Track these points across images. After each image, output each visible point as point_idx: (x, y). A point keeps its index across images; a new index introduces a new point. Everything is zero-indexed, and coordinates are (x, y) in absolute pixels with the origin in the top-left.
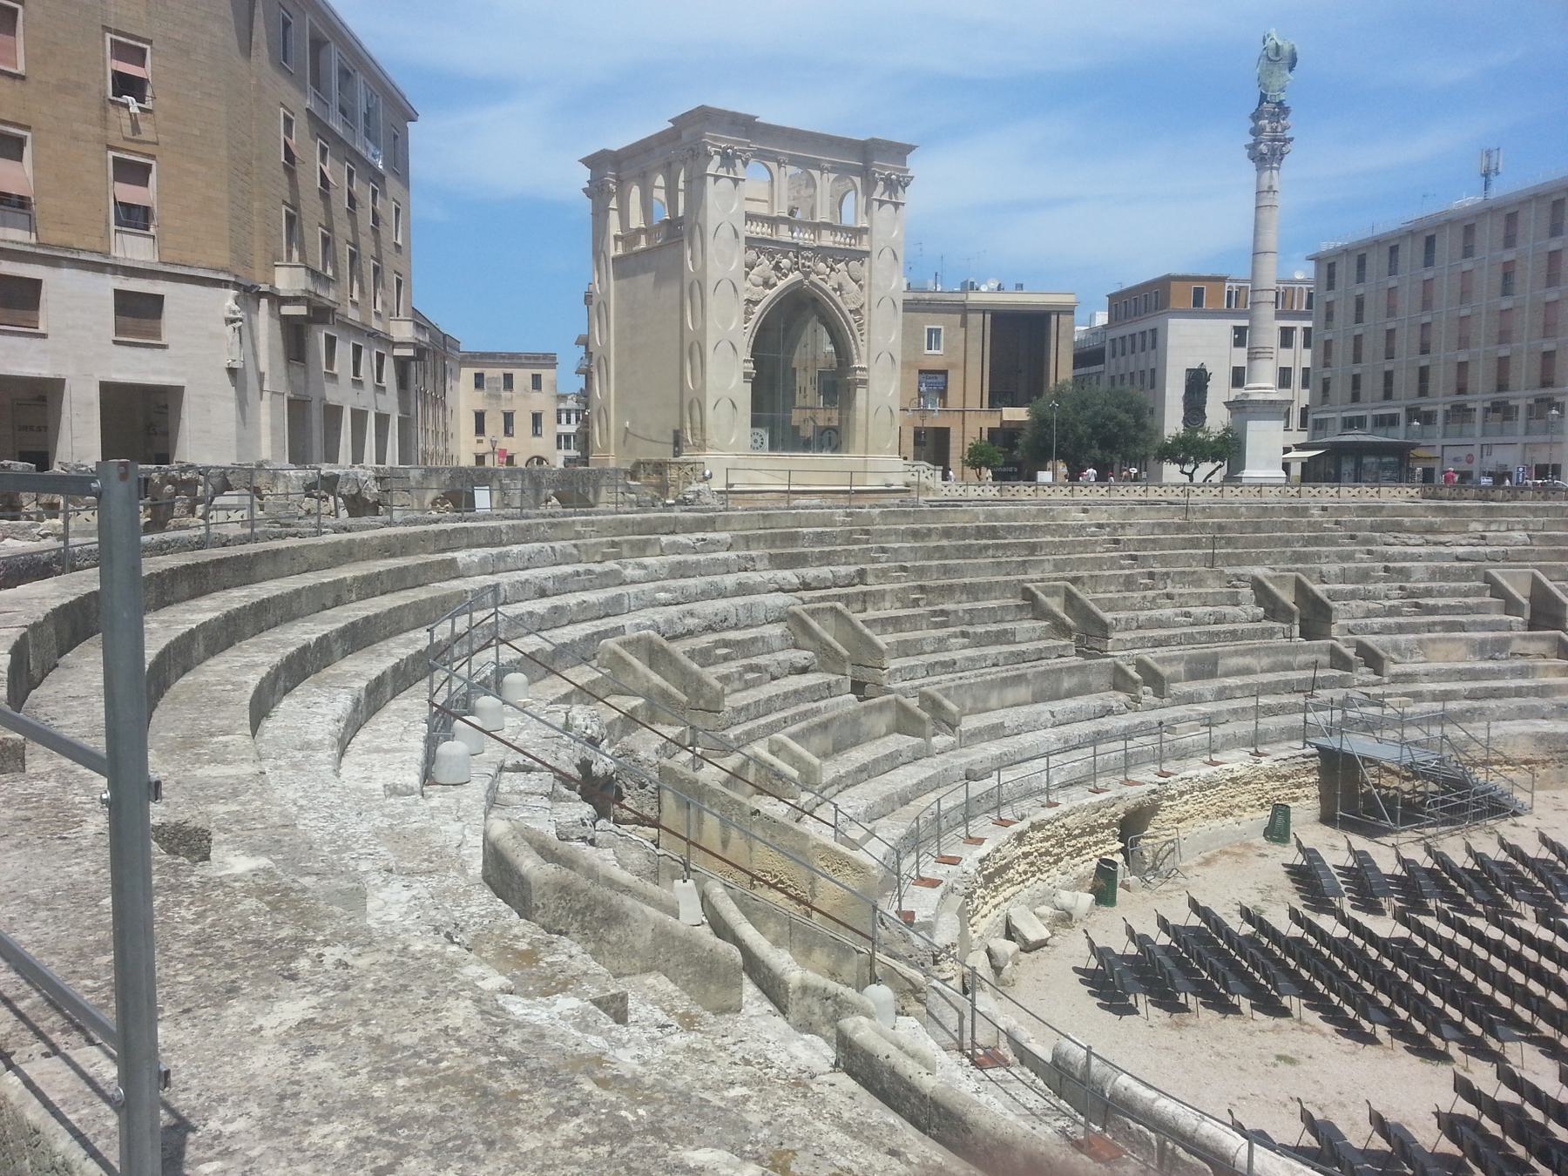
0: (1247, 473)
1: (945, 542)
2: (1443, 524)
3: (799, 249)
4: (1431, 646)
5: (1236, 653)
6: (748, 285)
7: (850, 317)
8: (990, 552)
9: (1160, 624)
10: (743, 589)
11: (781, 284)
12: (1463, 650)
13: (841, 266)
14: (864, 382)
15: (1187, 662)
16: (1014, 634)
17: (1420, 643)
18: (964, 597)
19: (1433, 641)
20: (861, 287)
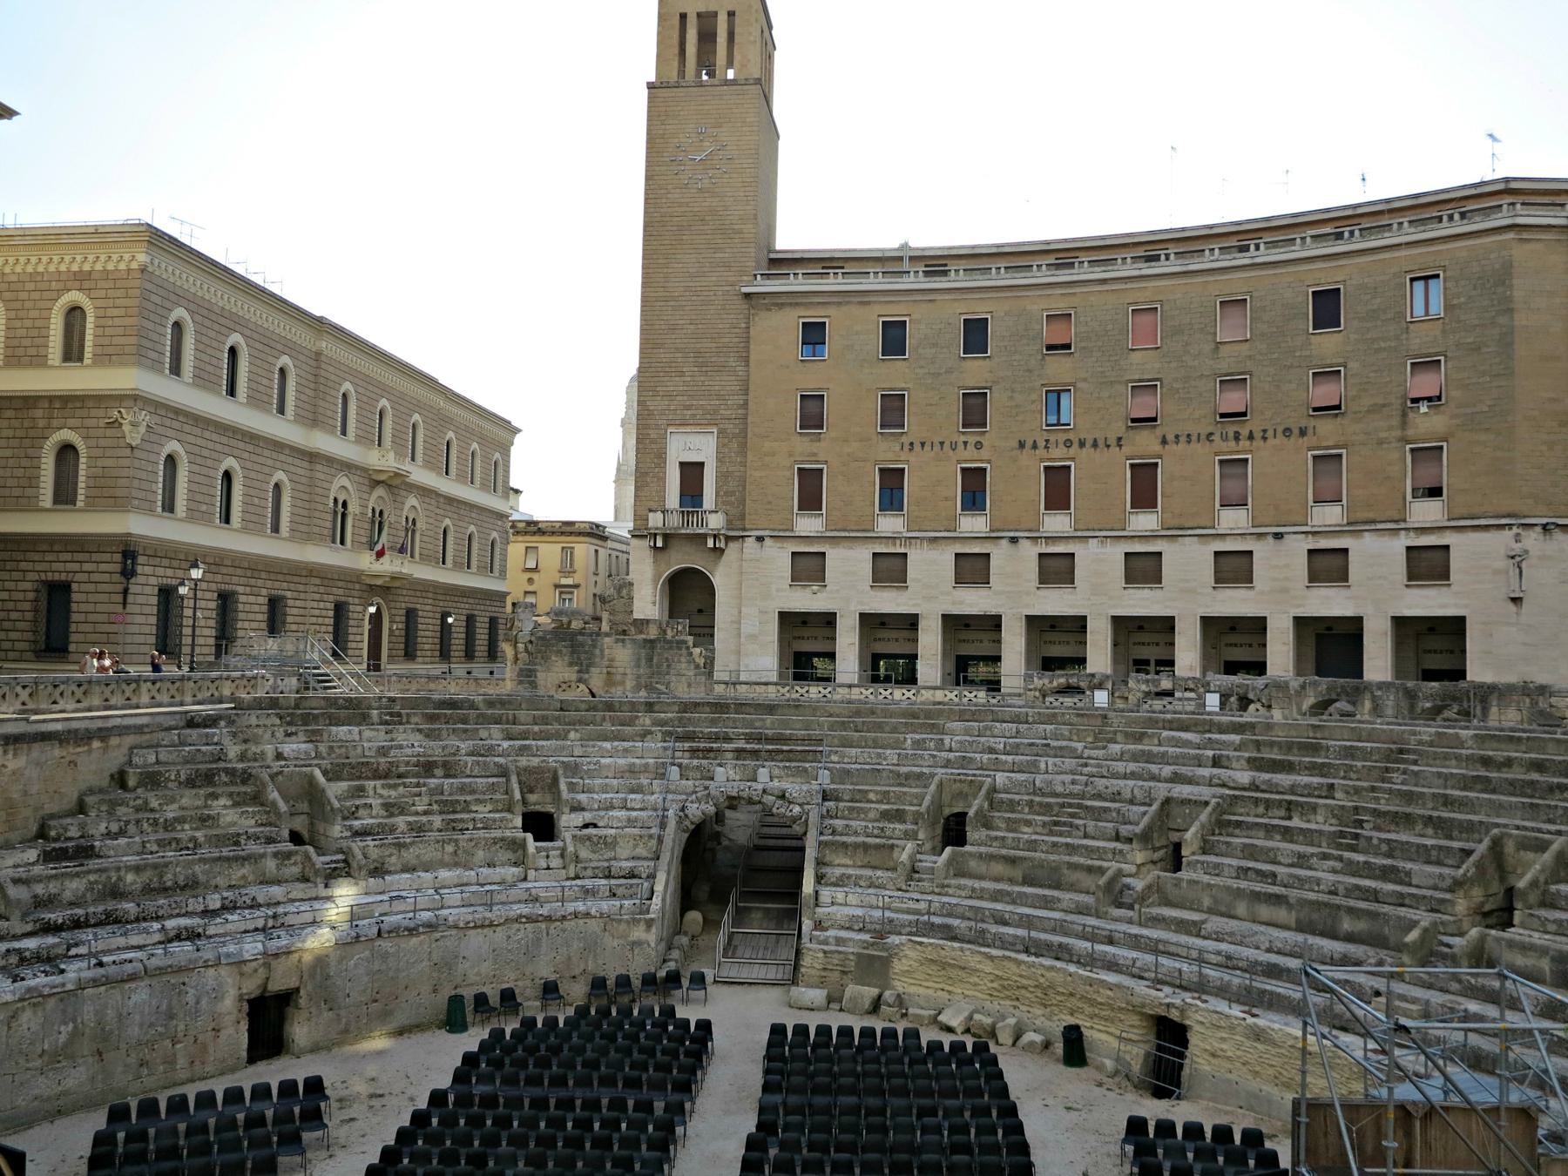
1: (1535, 776)
10: (1176, 778)
15: (1553, 959)
18: (1430, 831)
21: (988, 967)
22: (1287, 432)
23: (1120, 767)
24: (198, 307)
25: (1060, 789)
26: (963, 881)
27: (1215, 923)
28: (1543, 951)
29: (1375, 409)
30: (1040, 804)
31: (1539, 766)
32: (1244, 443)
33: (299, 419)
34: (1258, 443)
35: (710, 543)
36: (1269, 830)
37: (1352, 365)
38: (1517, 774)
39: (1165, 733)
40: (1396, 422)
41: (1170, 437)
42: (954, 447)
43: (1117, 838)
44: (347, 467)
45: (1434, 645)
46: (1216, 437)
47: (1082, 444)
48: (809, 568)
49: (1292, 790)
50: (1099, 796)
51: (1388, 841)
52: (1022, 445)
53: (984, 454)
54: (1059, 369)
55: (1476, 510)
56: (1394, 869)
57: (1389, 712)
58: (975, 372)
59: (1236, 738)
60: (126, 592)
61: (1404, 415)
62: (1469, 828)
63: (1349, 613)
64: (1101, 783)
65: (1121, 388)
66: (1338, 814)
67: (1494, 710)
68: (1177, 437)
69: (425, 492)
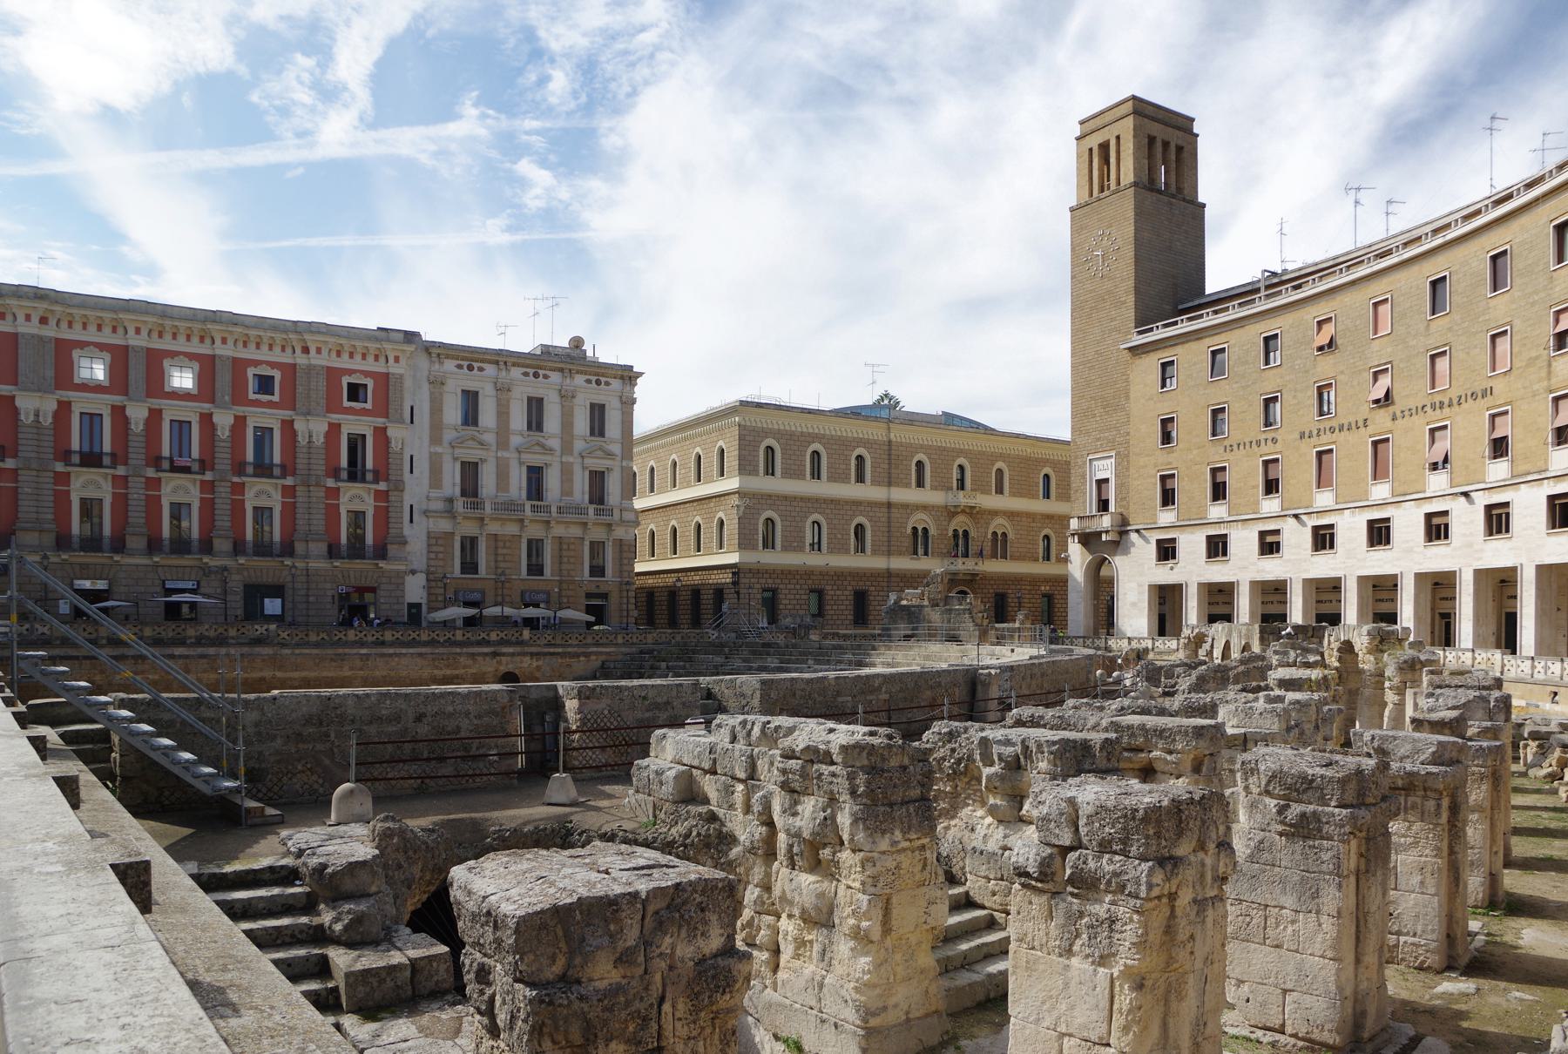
24: (778, 434)
32: (1446, 410)
33: (875, 483)
35: (1104, 538)
41: (1399, 414)
42: (1258, 443)
44: (925, 508)
46: (1428, 409)
48: (1166, 551)
52: (1302, 436)
53: (1279, 447)
54: (1326, 367)
58: (1270, 383)
60: (738, 593)
65: (1365, 374)
69: (1011, 515)
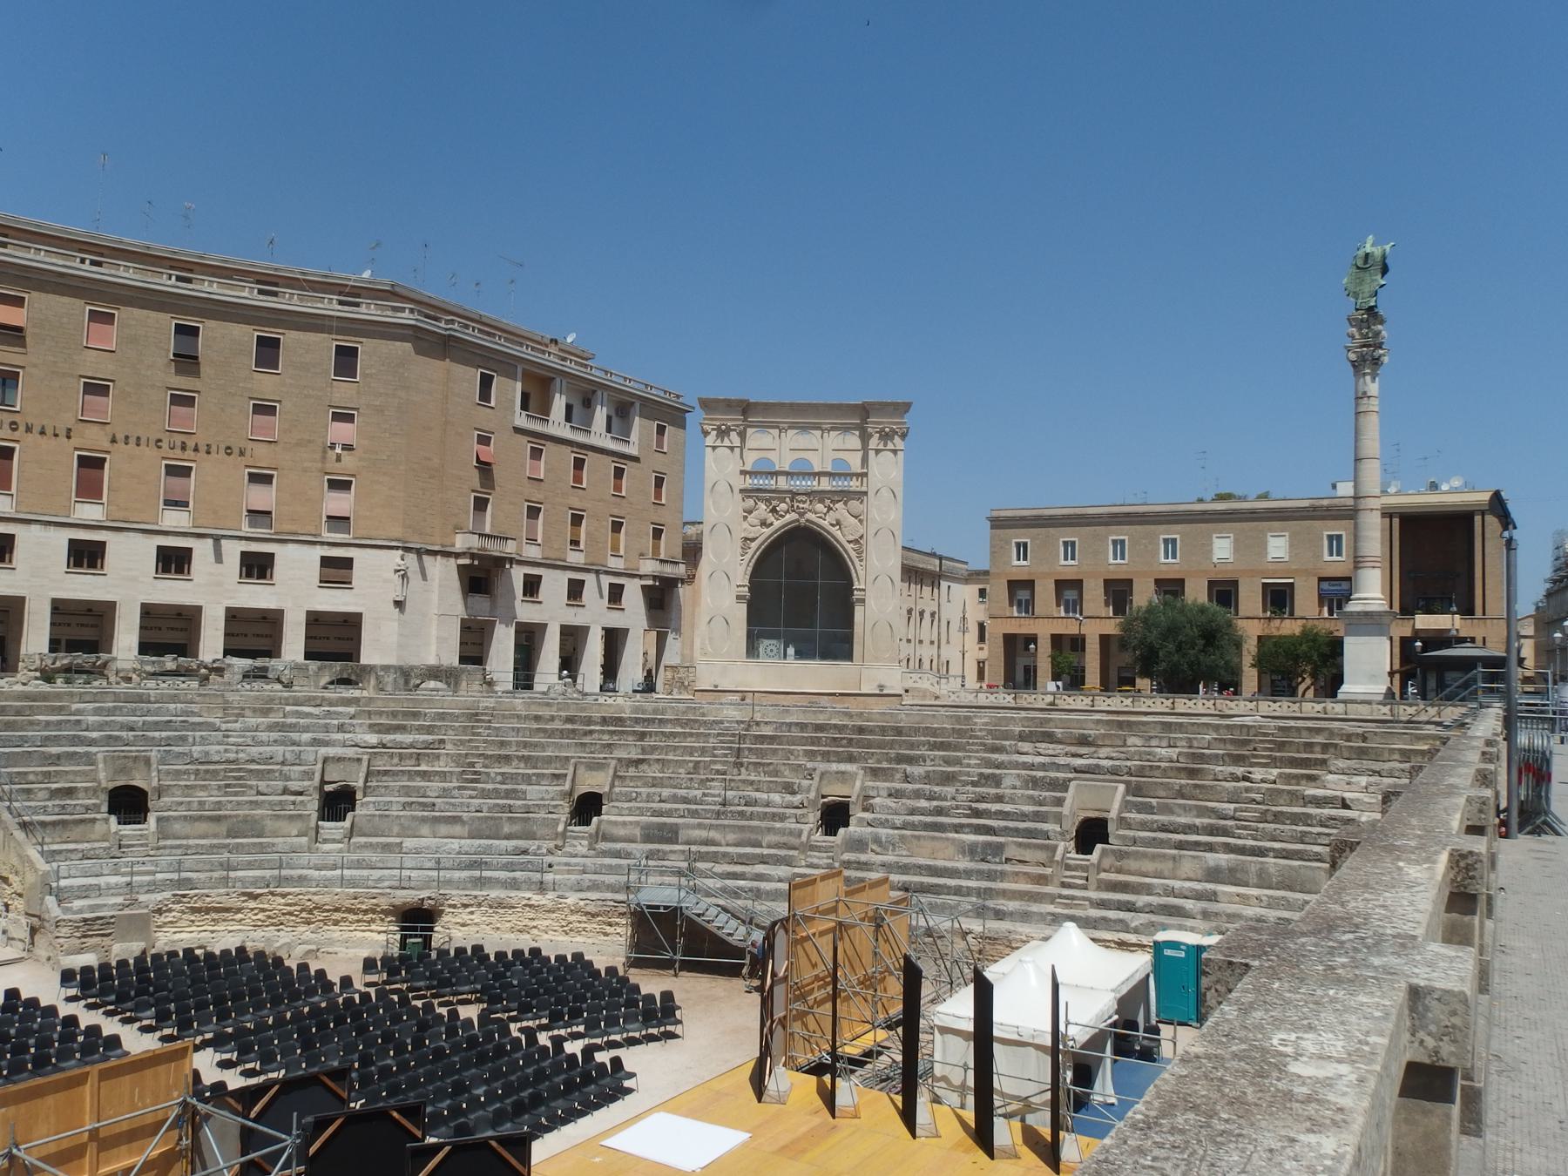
0: (1345, 688)
2: (1097, 737)
3: (794, 495)
4: (915, 842)
5: (700, 826)
6: (745, 525)
7: (849, 547)
8: (596, 736)
9: (685, 800)
10: (316, 742)
11: (777, 524)
12: (951, 850)
13: (839, 505)
14: (863, 601)
16: (525, 792)
17: (902, 837)
19: (918, 838)
20: (861, 521)
21: (252, 904)
22: (229, 450)
23: (264, 736)
25: (217, 758)
26: (169, 842)
27: (409, 843)
28: (637, 823)
29: (300, 444)
30: (207, 771)
31: (569, 720)
32: (189, 454)
34: (202, 454)
36: (411, 775)
37: (287, 404)
38: (557, 725)
39: (288, 708)
40: (318, 456)
41: (120, 437)
43: (285, 791)
45: (335, 639)
46: (165, 445)
47: (29, 429)
49: (412, 746)
50: (253, 761)
51: (503, 774)
55: (374, 533)
56: (515, 791)
57: (389, 688)
59: (352, 710)
61: (325, 452)
62: (549, 761)
63: (273, 606)
64: (254, 751)
66: (456, 759)
67: (464, 684)
68: (127, 437)
